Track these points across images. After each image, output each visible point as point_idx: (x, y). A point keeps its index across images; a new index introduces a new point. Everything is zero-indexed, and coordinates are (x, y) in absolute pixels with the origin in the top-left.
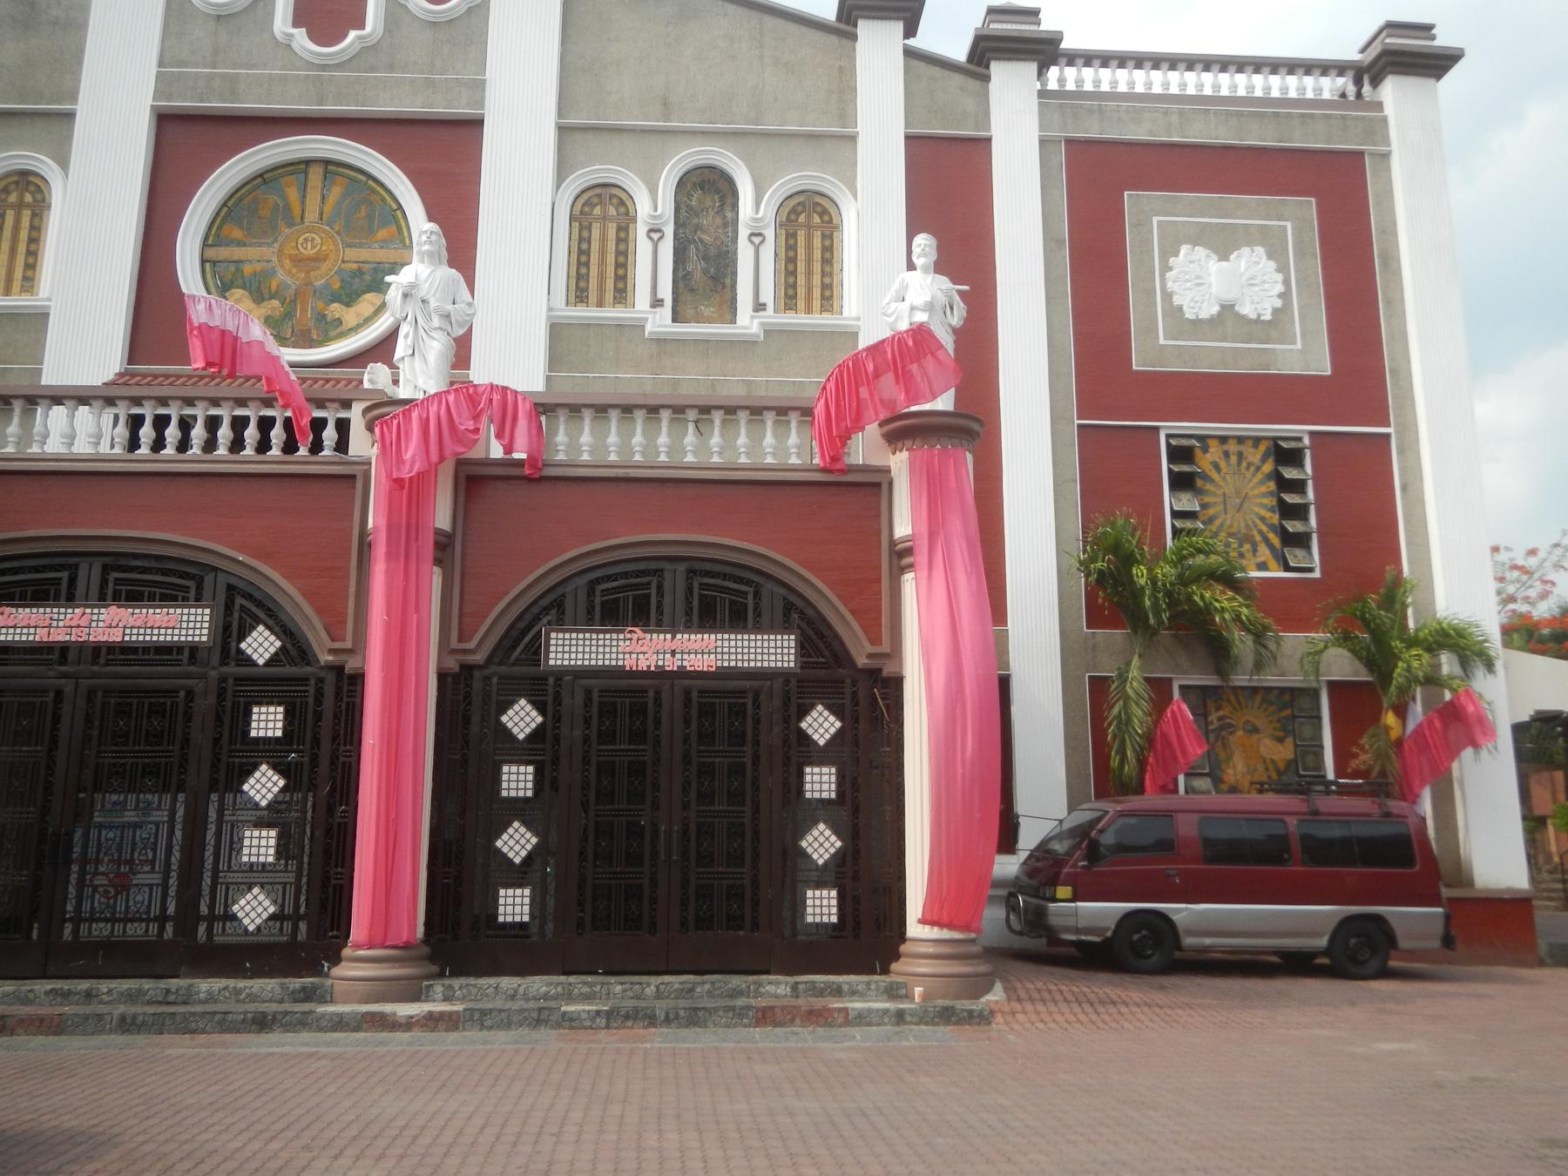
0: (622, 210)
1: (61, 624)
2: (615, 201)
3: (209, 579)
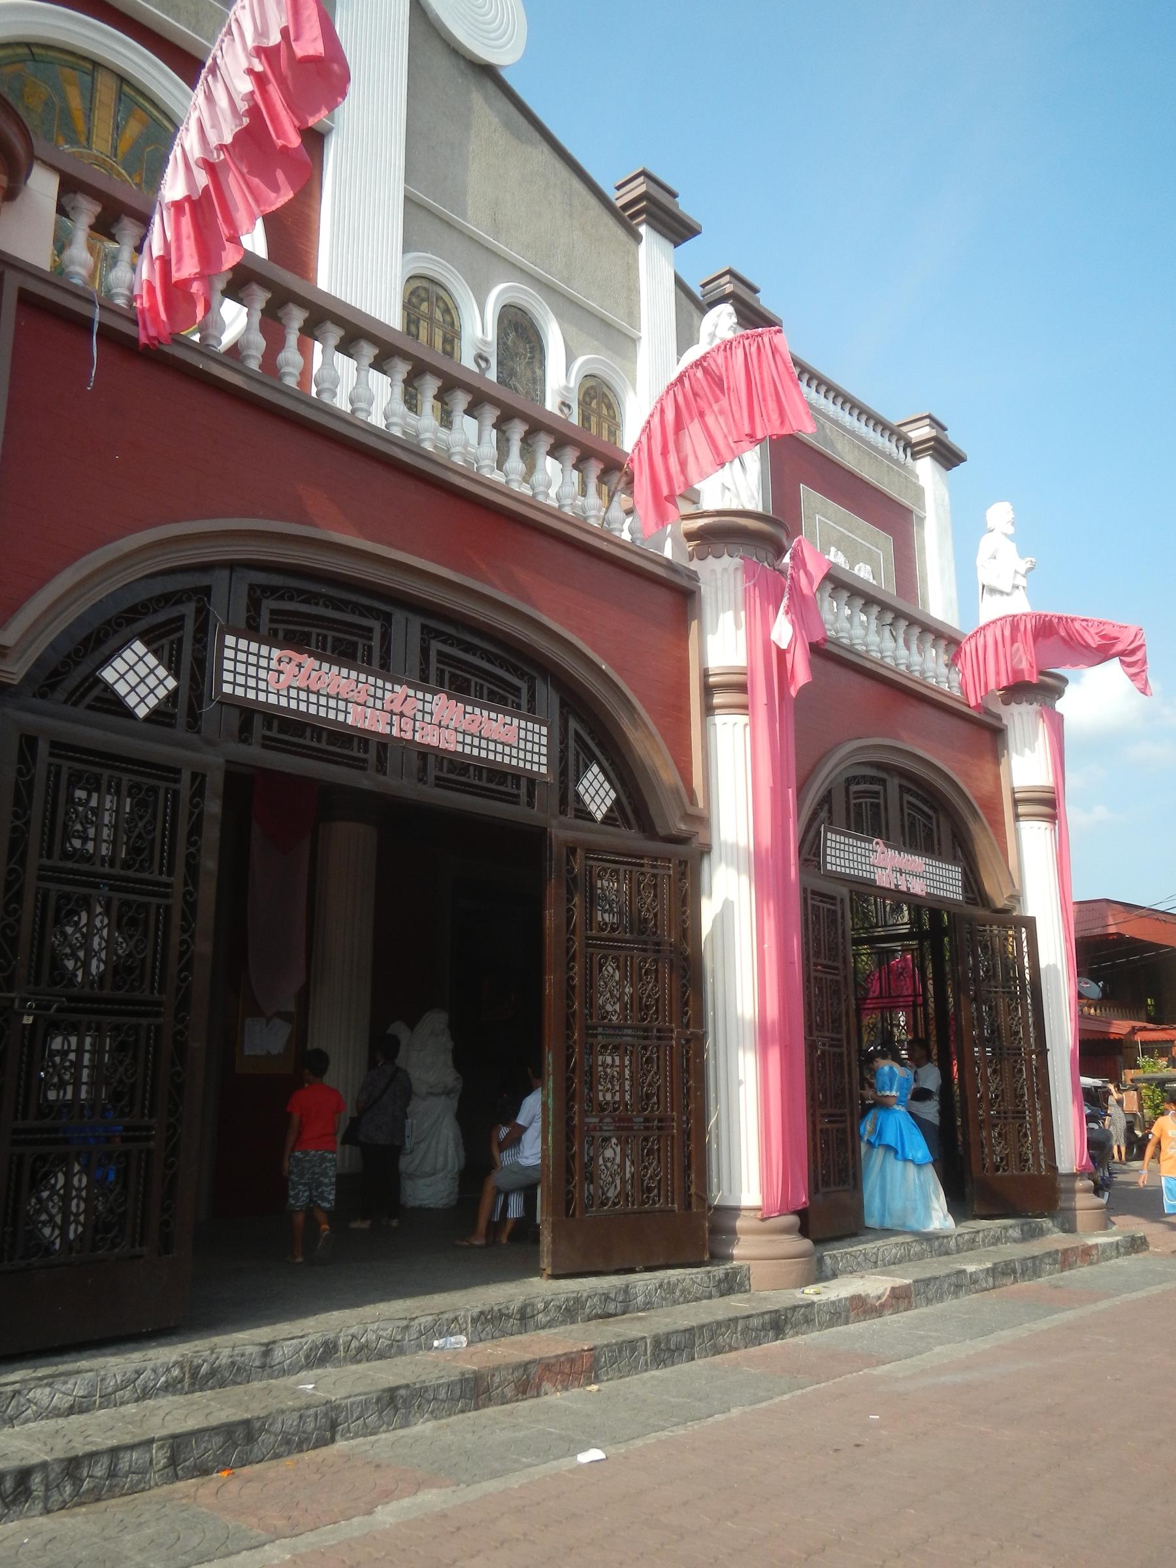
0: (448, 318)
1: (379, 704)
2: (441, 305)
3: (539, 685)
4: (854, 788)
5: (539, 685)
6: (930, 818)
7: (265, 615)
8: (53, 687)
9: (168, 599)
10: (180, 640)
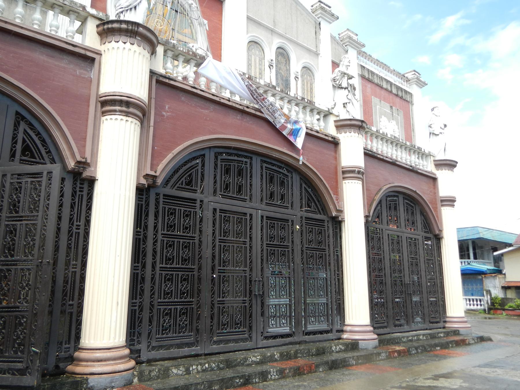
0: (260, 54)
4: (388, 199)
5: (294, 175)
6: (412, 207)
7: (219, 161)
8: (167, 185)
9: (195, 158)
10: (198, 169)
